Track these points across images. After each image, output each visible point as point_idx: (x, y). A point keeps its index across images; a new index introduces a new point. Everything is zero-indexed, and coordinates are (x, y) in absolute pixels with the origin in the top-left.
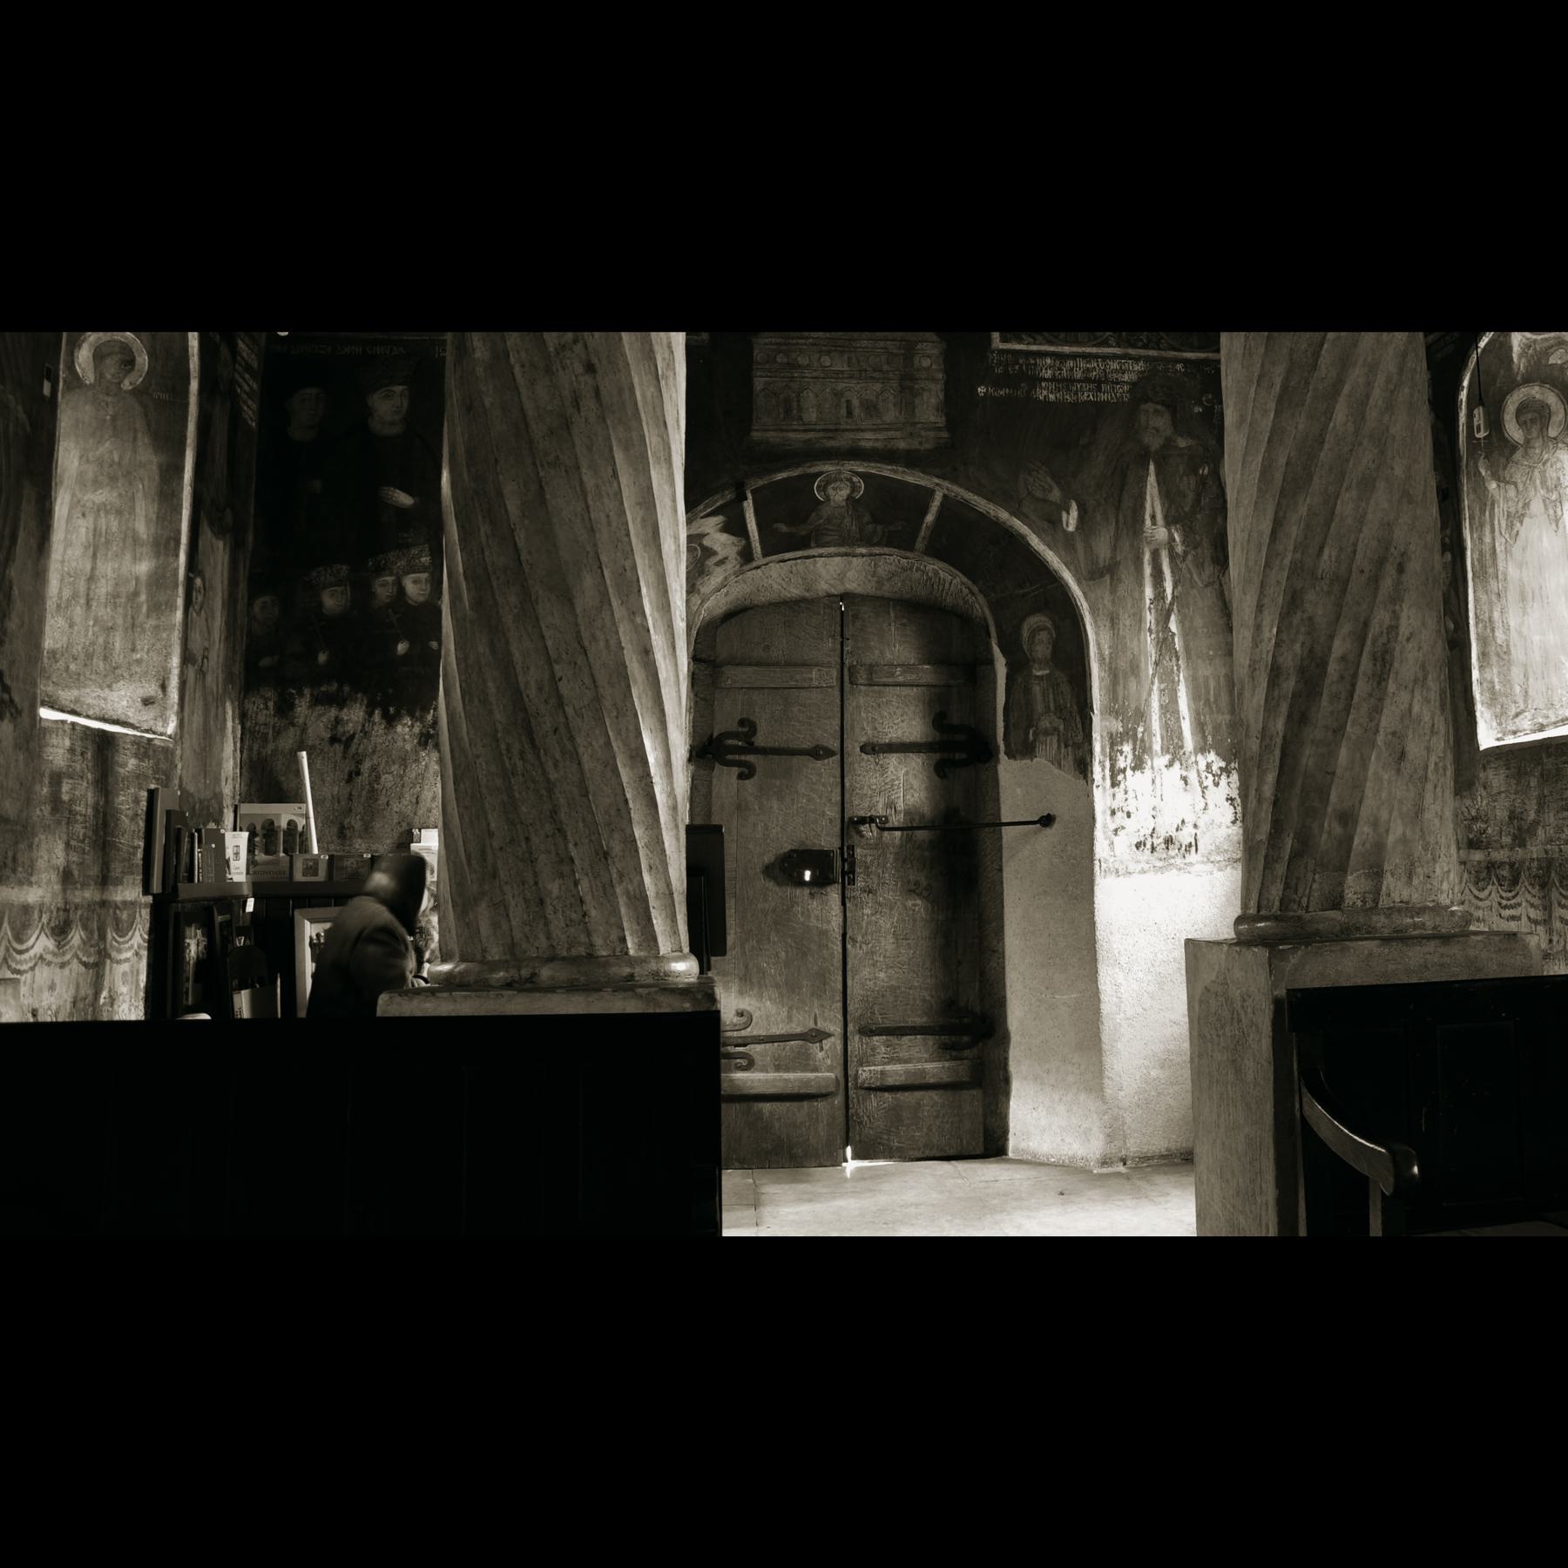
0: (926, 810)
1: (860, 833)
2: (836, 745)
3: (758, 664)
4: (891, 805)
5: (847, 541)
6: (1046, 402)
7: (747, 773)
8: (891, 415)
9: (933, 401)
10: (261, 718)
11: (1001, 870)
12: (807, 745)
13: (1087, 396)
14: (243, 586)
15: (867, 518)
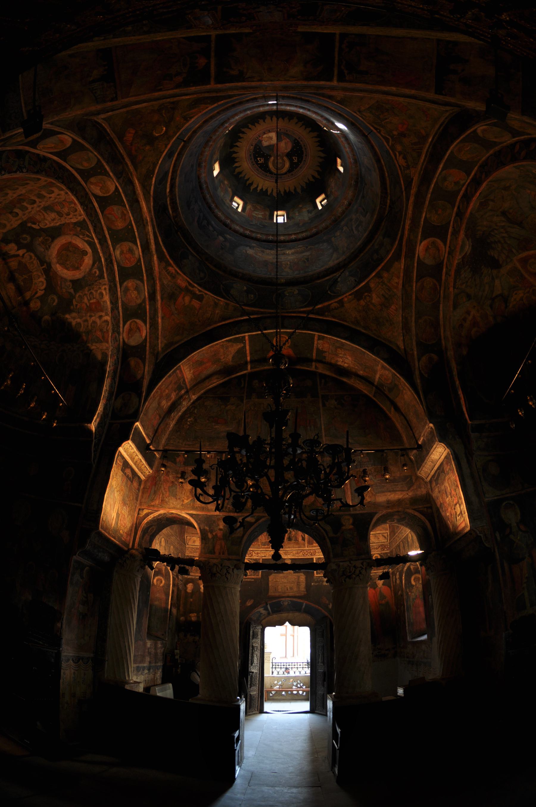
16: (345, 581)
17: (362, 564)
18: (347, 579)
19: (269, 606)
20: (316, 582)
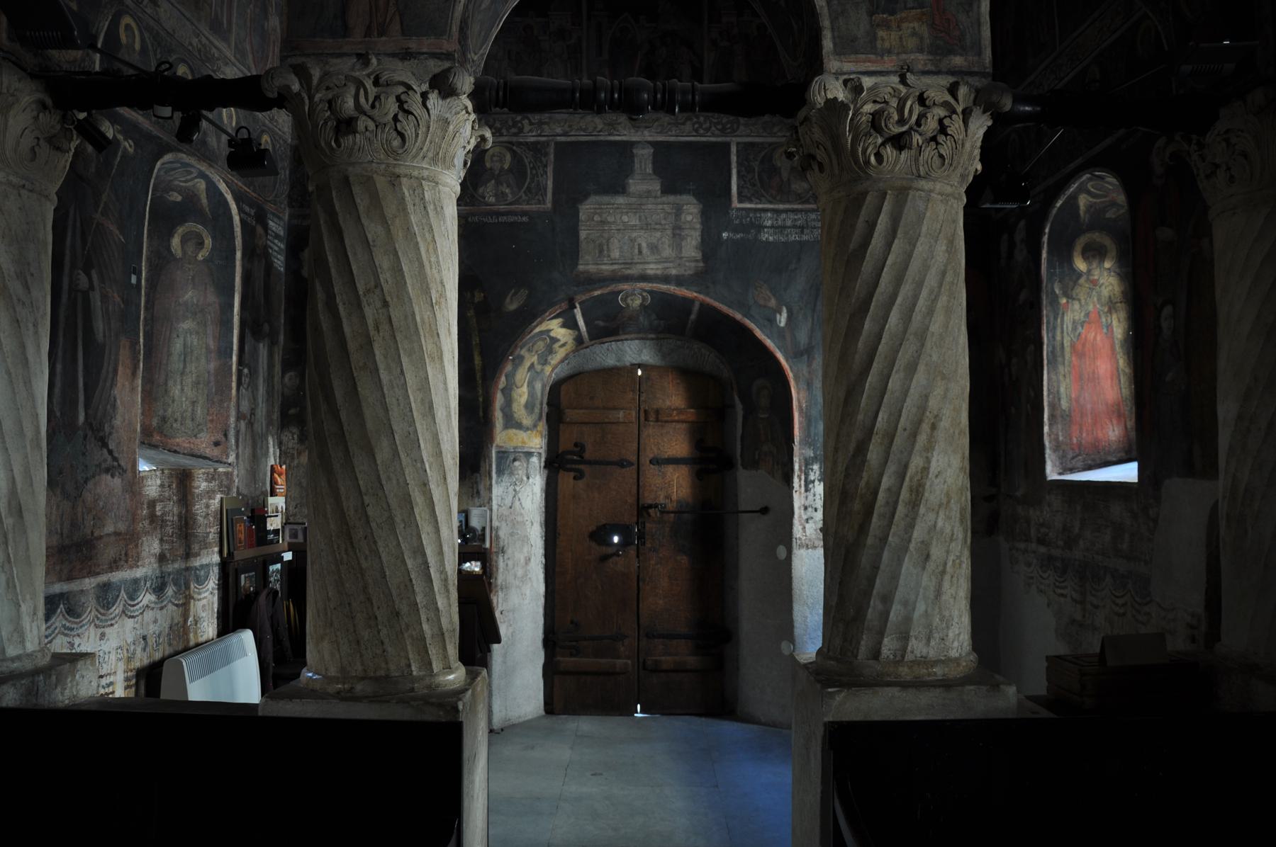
1: (649, 515)
2: (633, 458)
3: (586, 408)
4: (668, 497)
5: (642, 334)
6: (767, 242)
8: (667, 252)
9: (694, 243)
10: (290, 445)
11: (737, 538)
13: (794, 237)
14: (278, 368)
15: (654, 317)
19: (578, 312)
20: (735, 231)
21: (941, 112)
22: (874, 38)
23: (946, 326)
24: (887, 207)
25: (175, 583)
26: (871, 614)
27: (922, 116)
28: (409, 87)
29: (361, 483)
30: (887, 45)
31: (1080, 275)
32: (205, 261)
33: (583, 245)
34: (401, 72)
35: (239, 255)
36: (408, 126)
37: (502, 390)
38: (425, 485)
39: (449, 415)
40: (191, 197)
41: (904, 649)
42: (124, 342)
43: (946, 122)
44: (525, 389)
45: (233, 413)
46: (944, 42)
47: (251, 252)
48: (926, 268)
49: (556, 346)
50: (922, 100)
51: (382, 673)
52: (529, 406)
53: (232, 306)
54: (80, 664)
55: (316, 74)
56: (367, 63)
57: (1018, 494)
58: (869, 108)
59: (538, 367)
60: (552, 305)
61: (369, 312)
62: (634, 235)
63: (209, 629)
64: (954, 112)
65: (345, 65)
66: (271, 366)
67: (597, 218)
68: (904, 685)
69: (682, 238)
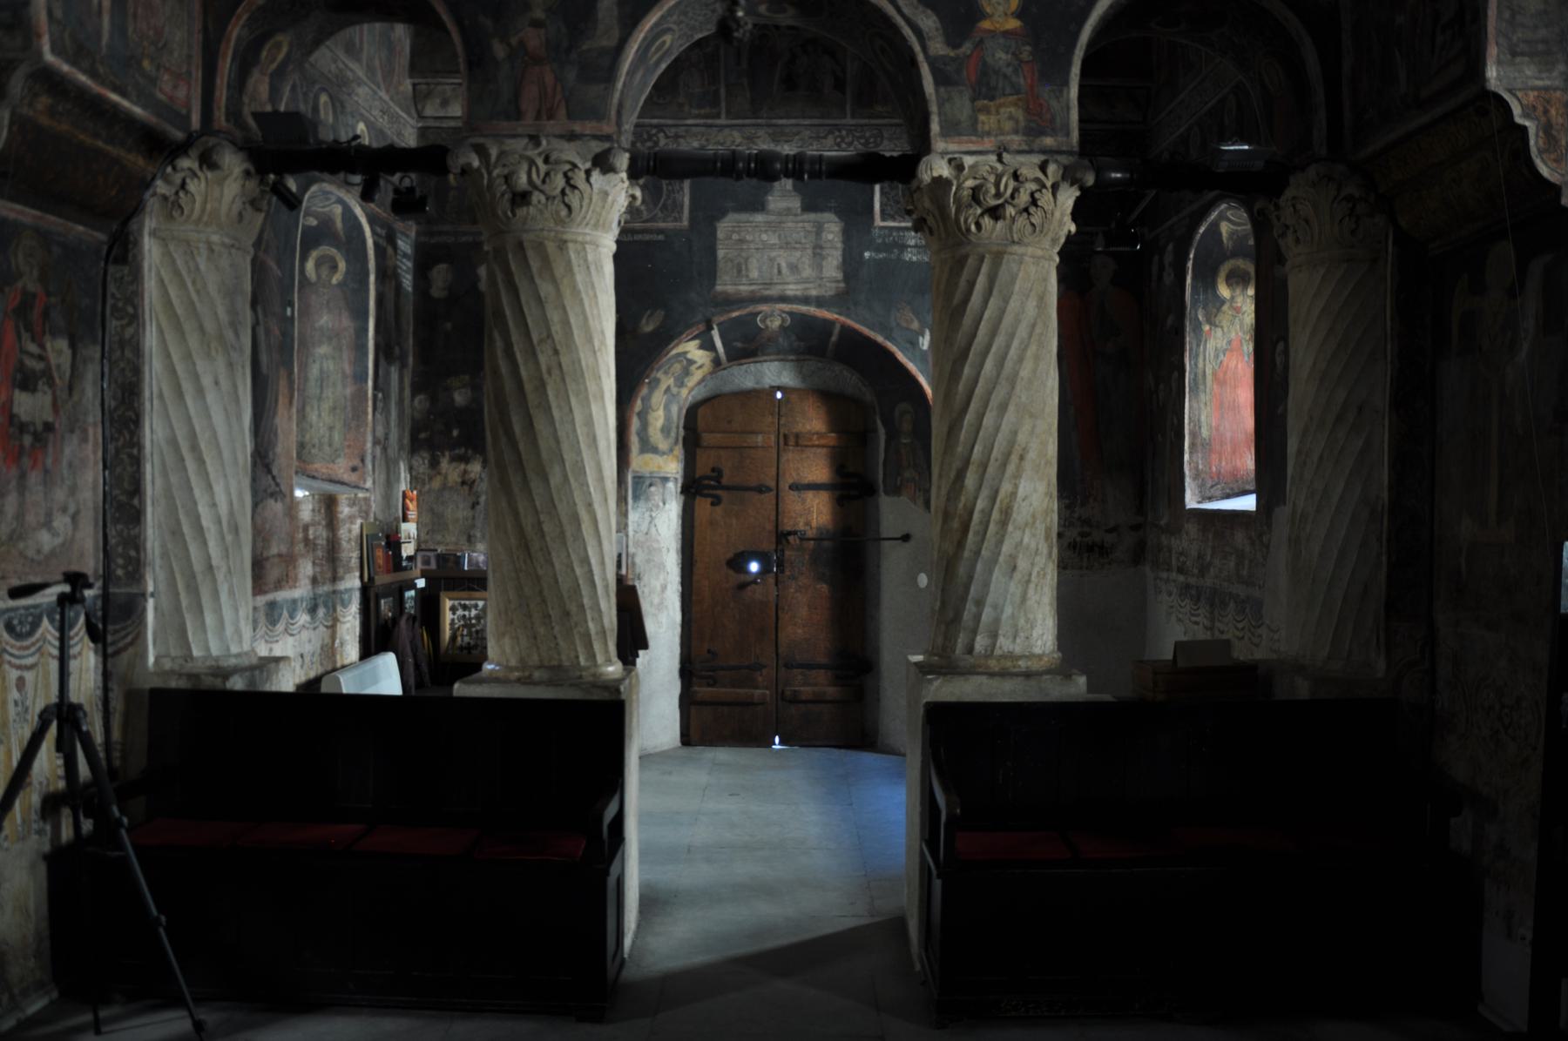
0: (830, 527)
2: (772, 484)
4: (808, 524)
5: (781, 354)
6: (911, 263)
7: (716, 501)
8: (807, 272)
9: (835, 263)
12: (754, 484)
14: (407, 392)
15: (794, 338)
16: (978, 226)
17: (1043, 167)
18: (987, 221)
19: (716, 334)
20: (878, 250)
21: (1033, 186)
22: (975, 121)
23: (1034, 371)
24: (985, 269)
25: (324, 605)
26: (967, 616)
27: (1016, 190)
28: (575, 166)
29: (538, 503)
30: (987, 128)
31: (1223, 302)
32: (341, 285)
33: (721, 265)
34: (569, 152)
35: (372, 278)
36: (573, 199)
37: (639, 414)
38: (590, 505)
39: (609, 447)
40: (326, 222)
41: (994, 645)
42: (283, 372)
43: (1037, 195)
44: (661, 413)
45: (369, 438)
46: (1037, 125)
47: (387, 274)
48: (1017, 321)
49: (693, 368)
50: (1016, 176)
51: (555, 663)
52: (665, 430)
53: (366, 330)
54: (282, 665)
55: (494, 152)
56: (538, 144)
57: (1162, 523)
58: (970, 183)
59: (675, 390)
60: (688, 327)
61: (543, 359)
62: (773, 254)
63: (352, 652)
64: (1044, 186)
65: (519, 145)
66: (401, 389)
67: (735, 237)
68: (992, 675)
69: (823, 258)
